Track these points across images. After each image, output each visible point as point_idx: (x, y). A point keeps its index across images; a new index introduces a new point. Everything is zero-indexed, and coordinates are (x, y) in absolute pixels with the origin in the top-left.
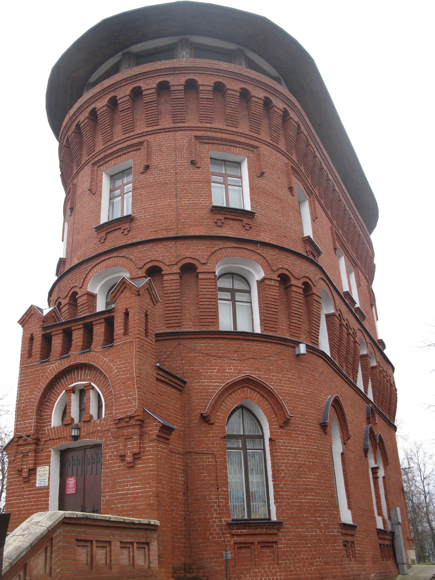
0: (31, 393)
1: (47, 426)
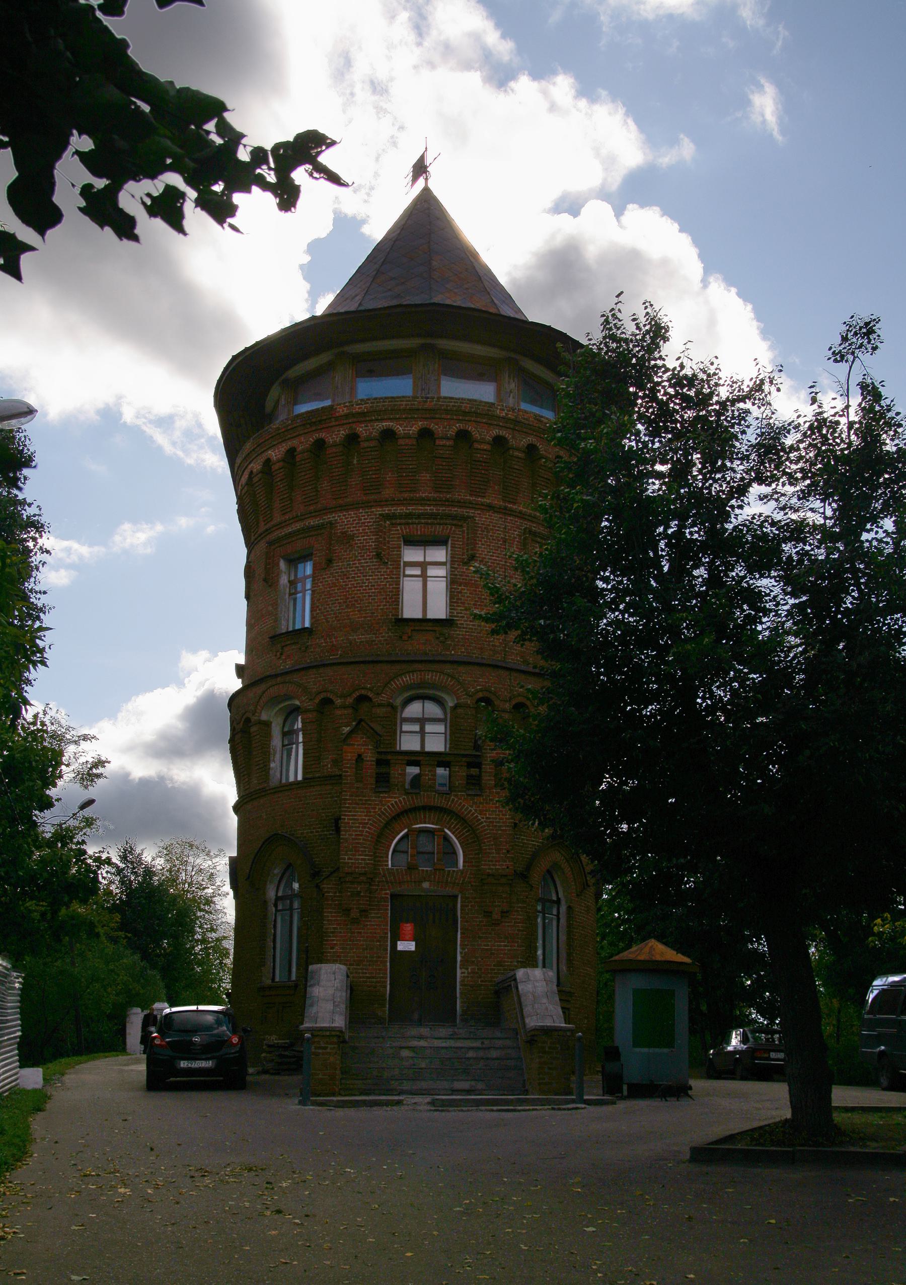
1: (382, 865)
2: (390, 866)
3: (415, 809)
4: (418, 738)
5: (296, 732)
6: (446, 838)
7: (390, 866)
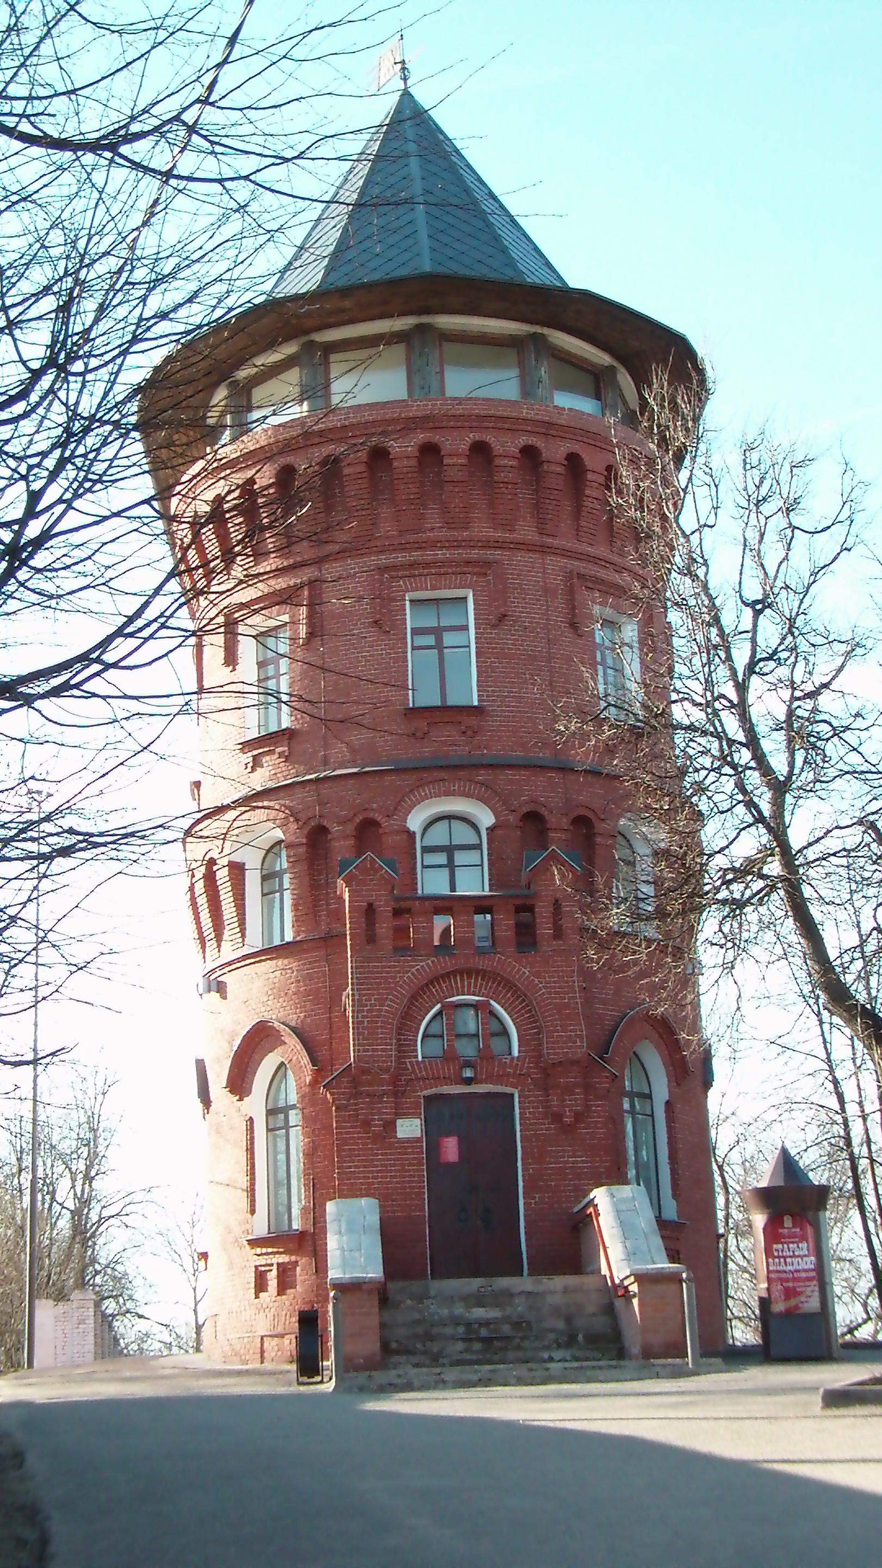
0: (381, 1001)
1: (410, 1057)
2: (420, 1058)
3: (447, 976)
4: (444, 874)
5: (279, 875)
6: (493, 1014)
7: (420, 1058)
